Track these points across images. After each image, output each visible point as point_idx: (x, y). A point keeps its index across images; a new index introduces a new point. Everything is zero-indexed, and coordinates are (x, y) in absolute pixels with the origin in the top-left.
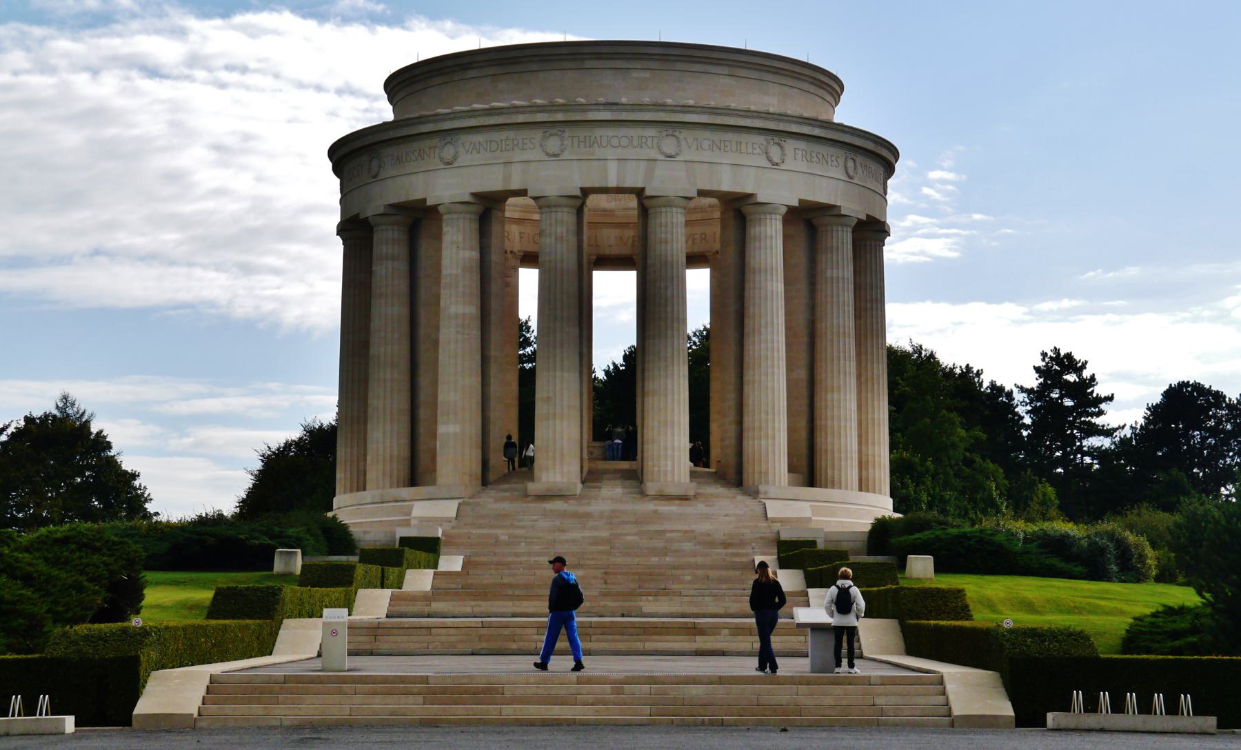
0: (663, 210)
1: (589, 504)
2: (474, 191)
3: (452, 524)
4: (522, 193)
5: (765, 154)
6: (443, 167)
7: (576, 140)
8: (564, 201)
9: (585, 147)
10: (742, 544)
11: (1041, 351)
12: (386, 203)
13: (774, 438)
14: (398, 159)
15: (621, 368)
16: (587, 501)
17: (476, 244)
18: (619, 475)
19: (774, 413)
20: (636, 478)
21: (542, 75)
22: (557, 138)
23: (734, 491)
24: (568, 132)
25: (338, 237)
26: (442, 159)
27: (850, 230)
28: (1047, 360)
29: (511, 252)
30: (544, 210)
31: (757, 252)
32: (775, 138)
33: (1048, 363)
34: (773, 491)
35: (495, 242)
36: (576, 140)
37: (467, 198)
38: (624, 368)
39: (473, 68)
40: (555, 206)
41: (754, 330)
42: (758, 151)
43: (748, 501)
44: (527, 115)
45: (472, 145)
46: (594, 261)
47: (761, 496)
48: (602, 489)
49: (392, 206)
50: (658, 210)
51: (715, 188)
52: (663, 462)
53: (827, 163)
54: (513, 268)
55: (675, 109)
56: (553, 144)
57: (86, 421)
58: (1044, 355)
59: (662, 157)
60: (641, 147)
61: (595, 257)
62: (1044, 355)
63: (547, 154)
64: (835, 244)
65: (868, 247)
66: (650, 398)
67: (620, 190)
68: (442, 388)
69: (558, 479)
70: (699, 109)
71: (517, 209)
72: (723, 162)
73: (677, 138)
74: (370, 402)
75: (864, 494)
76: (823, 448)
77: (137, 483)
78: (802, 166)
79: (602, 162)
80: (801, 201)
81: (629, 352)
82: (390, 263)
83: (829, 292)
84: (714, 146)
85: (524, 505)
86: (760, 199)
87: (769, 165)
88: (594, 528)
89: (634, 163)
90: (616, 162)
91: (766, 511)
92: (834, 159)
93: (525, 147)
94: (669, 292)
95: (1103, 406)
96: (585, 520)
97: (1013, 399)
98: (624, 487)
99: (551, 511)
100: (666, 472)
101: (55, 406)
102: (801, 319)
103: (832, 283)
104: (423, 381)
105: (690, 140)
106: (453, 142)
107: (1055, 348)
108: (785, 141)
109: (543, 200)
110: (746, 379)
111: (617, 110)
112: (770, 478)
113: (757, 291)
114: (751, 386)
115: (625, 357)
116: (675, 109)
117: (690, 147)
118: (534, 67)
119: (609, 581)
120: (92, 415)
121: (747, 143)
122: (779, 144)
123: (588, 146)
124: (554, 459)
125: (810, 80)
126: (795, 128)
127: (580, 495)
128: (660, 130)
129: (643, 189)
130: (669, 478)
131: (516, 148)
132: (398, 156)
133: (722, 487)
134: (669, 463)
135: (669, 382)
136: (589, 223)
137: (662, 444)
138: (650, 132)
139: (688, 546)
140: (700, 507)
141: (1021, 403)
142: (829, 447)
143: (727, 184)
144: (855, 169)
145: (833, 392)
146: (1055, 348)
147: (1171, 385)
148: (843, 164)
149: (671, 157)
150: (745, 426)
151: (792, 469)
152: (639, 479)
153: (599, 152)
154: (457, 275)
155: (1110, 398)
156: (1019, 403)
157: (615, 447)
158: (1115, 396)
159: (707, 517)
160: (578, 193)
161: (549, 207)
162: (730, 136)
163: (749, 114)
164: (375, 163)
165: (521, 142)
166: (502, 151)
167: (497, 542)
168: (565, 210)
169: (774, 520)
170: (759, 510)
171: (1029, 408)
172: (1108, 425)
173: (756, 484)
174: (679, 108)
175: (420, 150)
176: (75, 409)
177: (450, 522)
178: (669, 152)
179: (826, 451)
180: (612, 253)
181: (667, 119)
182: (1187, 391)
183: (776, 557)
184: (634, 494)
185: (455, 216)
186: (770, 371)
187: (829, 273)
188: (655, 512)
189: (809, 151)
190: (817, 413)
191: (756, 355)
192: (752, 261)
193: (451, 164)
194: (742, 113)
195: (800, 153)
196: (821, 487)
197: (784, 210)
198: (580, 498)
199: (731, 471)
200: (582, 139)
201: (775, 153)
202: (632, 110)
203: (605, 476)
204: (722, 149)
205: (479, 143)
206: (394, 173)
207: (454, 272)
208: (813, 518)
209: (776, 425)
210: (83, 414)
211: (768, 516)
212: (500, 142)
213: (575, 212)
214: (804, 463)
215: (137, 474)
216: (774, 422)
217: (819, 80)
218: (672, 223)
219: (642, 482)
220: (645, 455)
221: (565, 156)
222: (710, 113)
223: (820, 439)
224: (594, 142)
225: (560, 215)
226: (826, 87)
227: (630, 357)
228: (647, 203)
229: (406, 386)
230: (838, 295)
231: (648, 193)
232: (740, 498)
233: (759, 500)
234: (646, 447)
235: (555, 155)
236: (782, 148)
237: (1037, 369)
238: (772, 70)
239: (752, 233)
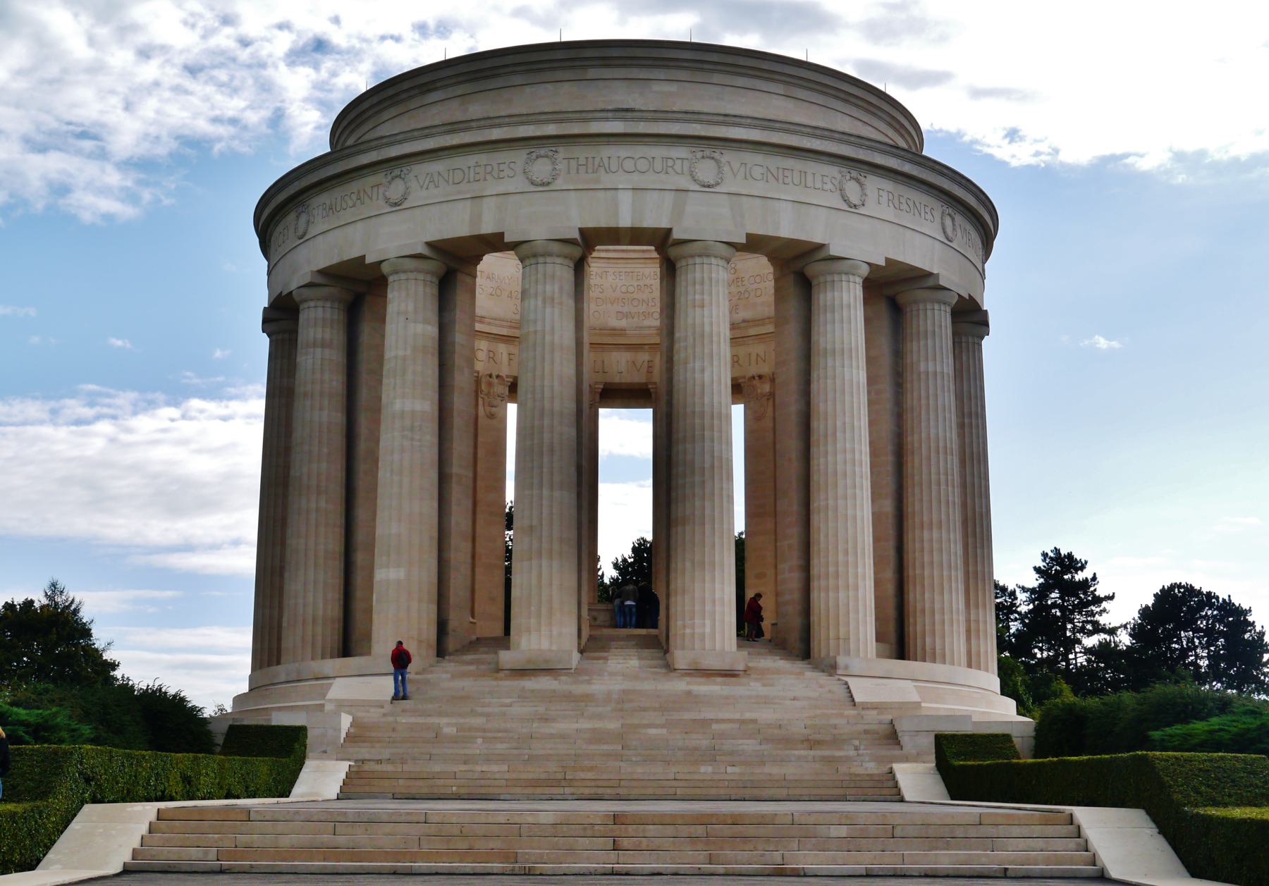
0: (698, 260)
1: (589, 682)
2: (430, 239)
3: (383, 711)
4: (495, 243)
5: (839, 192)
6: (390, 209)
7: (574, 163)
8: (556, 247)
9: (587, 172)
10: (837, 742)
11: (1042, 552)
12: (316, 269)
13: (856, 588)
14: (331, 209)
15: (630, 561)
16: (587, 678)
17: (433, 316)
18: (634, 643)
19: (857, 552)
20: (660, 646)
21: (528, 90)
22: (545, 160)
23: (799, 665)
24: (562, 152)
25: (265, 334)
26: (387, 200)
27: (949, 309)
28: (1048, 560)
29: (498, 376)
30: (527, 262)
31: (829, 327)
32: (852, 171)
33: (1049, 563)
34: (856, 665)
35: (460, 315)
36: (574, 163)
37: (421, 249)
38: (632, 560)
39: (436, 89)
40: (542, 255)
41: (826, 436)
42: (829, 186)
43: (823, 678)
44: (505, 129)
45: (429, 176)
46: (600, 390)
47: (839, 672)
48: (609, 661)
49: (323, 272)
50: (690, 261)
51: (770, 232)
52: (697, 621)
53: (920, 214)
54: (499, 396)
55: (716, 118)
56: (541, 169)
57: (75, 609)
58: (1045, 555)
59: (697, 188)
60: (667, 173)
61: (602, 387)
62: (1045, 555)
63: (533, 183)
64: (930, 328)
65: (964, 345)
66: (680, 529)
67: (636, 236)
68: (382, 516)
69: (545, 645)
70: (749, 121)
71: (505, 324)
72: (783, 197)
73: (717, 161)
74: (288, 542)
75: (973, 671)
76: (919, 606)
77: (118, 673)
78: (889, 214)
79: (610, 193)
80: (887, 260)
81: (638, 544)
82: (319, 350)
83: (923, 394)
84: (770, 175)
85: (495, 683)
86: (834, 251)
87: (845, 207)
88: (600, 717)
89: (656, 194)
90: (630, 193)
91: (848, 688)
92: (928, 210)
93: (502, 175)
94: (707, 375)
95: (1104, 604)
96: (583, 704)
97: (1016, 598)
98: (640, 658)
99: (533, 691)
100: (703, 636)
101: (44, 594)
102: (887, 426)
103: (928, 379)
104: (361, 514)
105: (736, 165)
106: (403, 176)
107: (1055, 548)
108: (865, 177)
109: (525, 246)
110: (814, 505)
111: (633, 119)
112: (852, 646)
113: (829, 381)
114: (822, 515)
115: (634, 549)
116: (716, 118)
117: (735, 176)
118: (517, 79)
119: (625, 843)
120: (80, 603)
121: (814, 174)
122: (857, 180)
123: (590, 170)
124: (539, 615)
125: (888, 119)
126: (879, 159)
127: (575, 669)
128: (694, 149)
129: (669, 231)
130: (708, 644)
131: (488, 177)
132: (331, 205)
133: (781, 659)
134: (708, 622)
135: (707, 504)
136: (591, 344)
137: (697, 595)
138: (681, 152)
139: (749, 745)
140: (753, 687)
141: (1024, 602)
142: (927, 606)
143: (786, 227)
144: (954, 229)
145: (931, 529)
146: (1055, 548)
147: (1164, 586)
148: (940, 220)
149: (709, 186)
150: (814, 571)
151: (879, 638)
152: (663, 648)
153: (607, 180)
154: (404, 358)
155: (1111, 598)
156: (1022, 603)
157: (627, 610)
158: (1116, 595)
159: (766, 701)
160: (576, 235)
161: (535, 256)
162: (790, 163)
163: (818, 132)
164: (303, 218)
165: (496, 167)
166: (469, 182)
167: (438, 736)
168: (559, 260)
169: (866, 707)
170: (840, 692)
171: (1031, 606)
172: (1110, 624)
173: (831, 654)
174: (721, 118)
175: (359, 192)
176: (63, 597)
177: (382, 707)
178: (706, 180)
179: (923, 611)
180: (623, 381)
181: (703, 133)
182: (1179, 592)
183: (934, 764)
184: (656, 667)
185: (403, 276)
186: (849, 491)
187: (922, 367)
188: (689, 693)
189: (896, 195)
190: (909, 557)
191: (830, 470)
192: (822, 340)
193: (399, 205)
194: (809, 130)
195: (884, 194)
196: (916, 660)
197: (865, 270)
198: (579, 672)
199: (794, 638)
200: (582, 161)
201: (852, 190)
202: (655, 120)
203: (613, 643)
204: (781, 181)
205: (439, 172)
206: (326, 227)
207: (401, 353)
208: (923, 705)
209: (860, 570)
210: (72, 602)
211: (857, 699)
212: (466, 171)
213: (572, 265)
214: (891, 628)
215: (117, 663)
216: (856, 567)
217: (899, 122)
218: (710, 279)
219: (667, 651)
220: (672, 610)
221: (559, 184)
222: (765, 128)
223: (913, 596)
224: (599, 166)
225: (549, 268)
226: (906, 136)
227: (640, 549)
228: (673, 252)
229: (337, 518)
230: (936, 395)
231: (677, 235)
232: (810, 674)
233: (837, 677)
234: (672, 600)
235: (543, 184)
236: (861, 185)
237: (1037, 570)
238: (842, 95)
239: (821, 303)
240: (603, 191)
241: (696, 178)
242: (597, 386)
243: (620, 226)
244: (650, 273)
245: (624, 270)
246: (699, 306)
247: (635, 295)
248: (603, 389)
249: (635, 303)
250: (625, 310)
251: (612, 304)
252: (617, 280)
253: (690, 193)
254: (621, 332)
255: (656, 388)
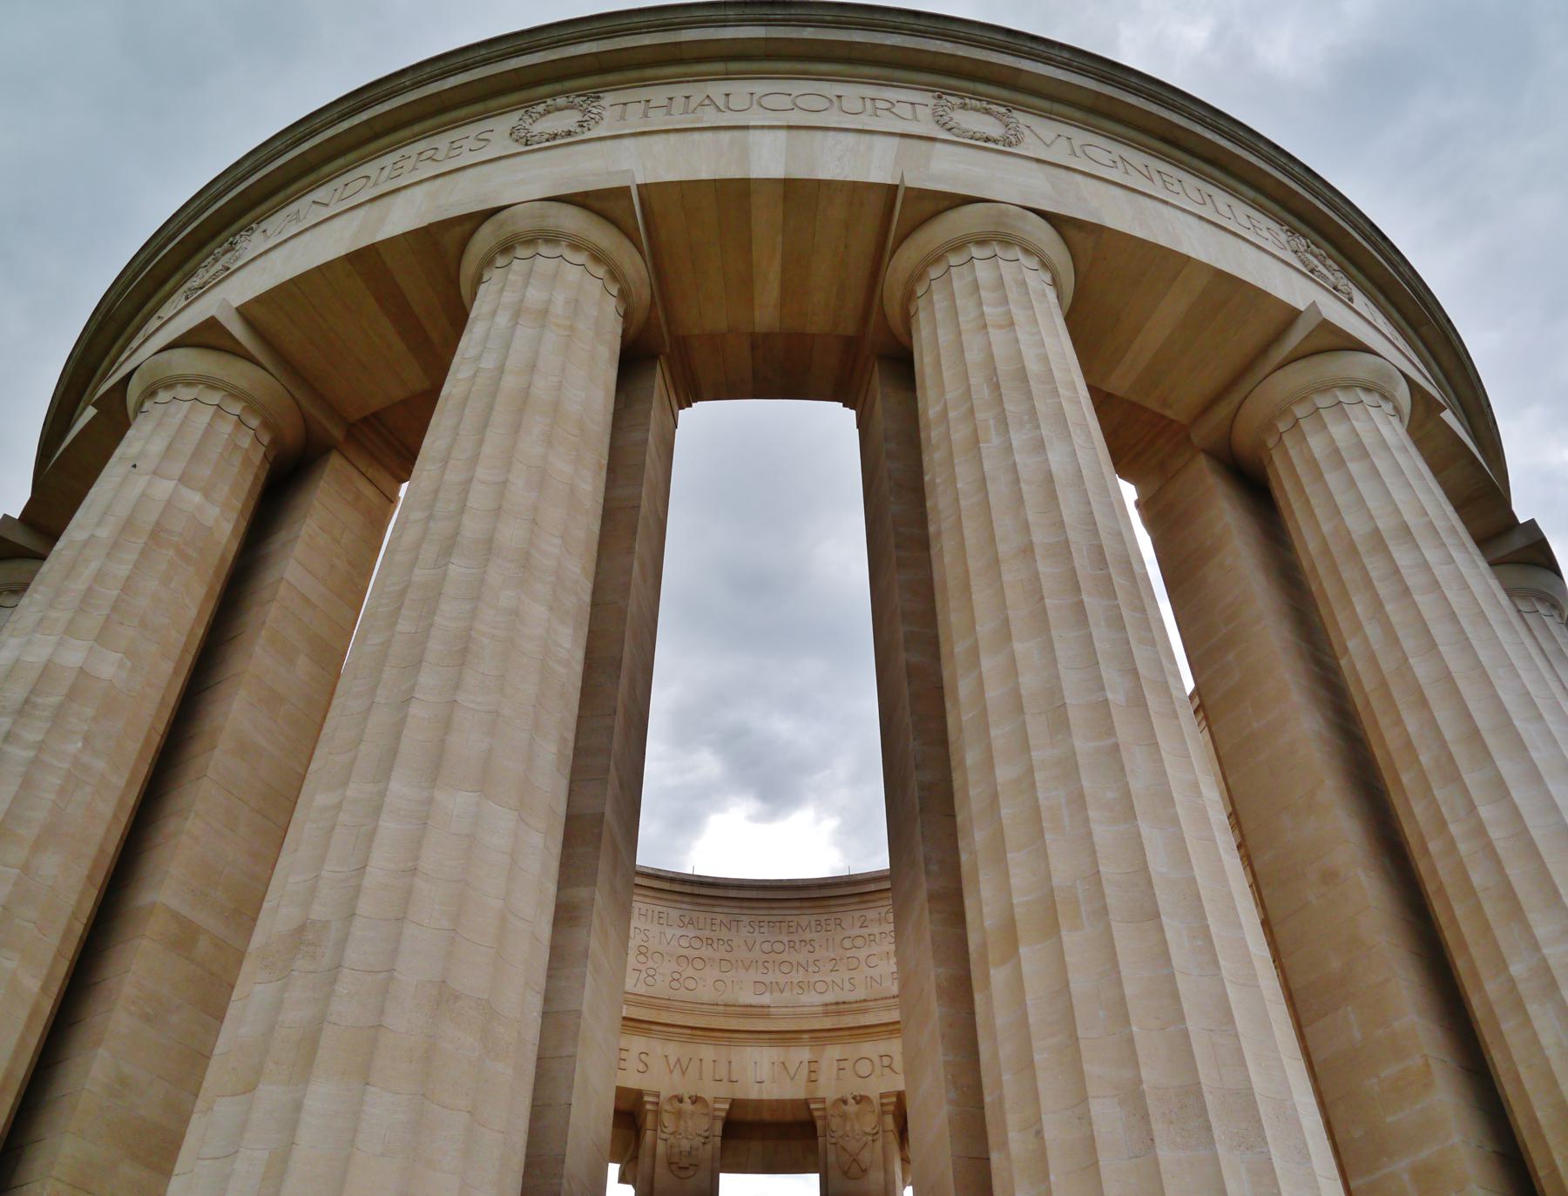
8: (572, 220)
90: (782, 134)
149: (987, 140)
161: (507, 248)
180: (765, 1096)
225: (544, 265)
240: (709, 135)
241: (952, 124)
242: (717, 1106)
243: (753, 175)
244: (810, 922)
245: (768, 918)
246: (1001, 327)
247: (784, 957)
248: (729, 1112)
249: (785, 968)
250: (768, 979)
251: (747, 970)
252: (756, 934)
253: (938, 146)
254: (762, 1012)
255: (824, 1109)
